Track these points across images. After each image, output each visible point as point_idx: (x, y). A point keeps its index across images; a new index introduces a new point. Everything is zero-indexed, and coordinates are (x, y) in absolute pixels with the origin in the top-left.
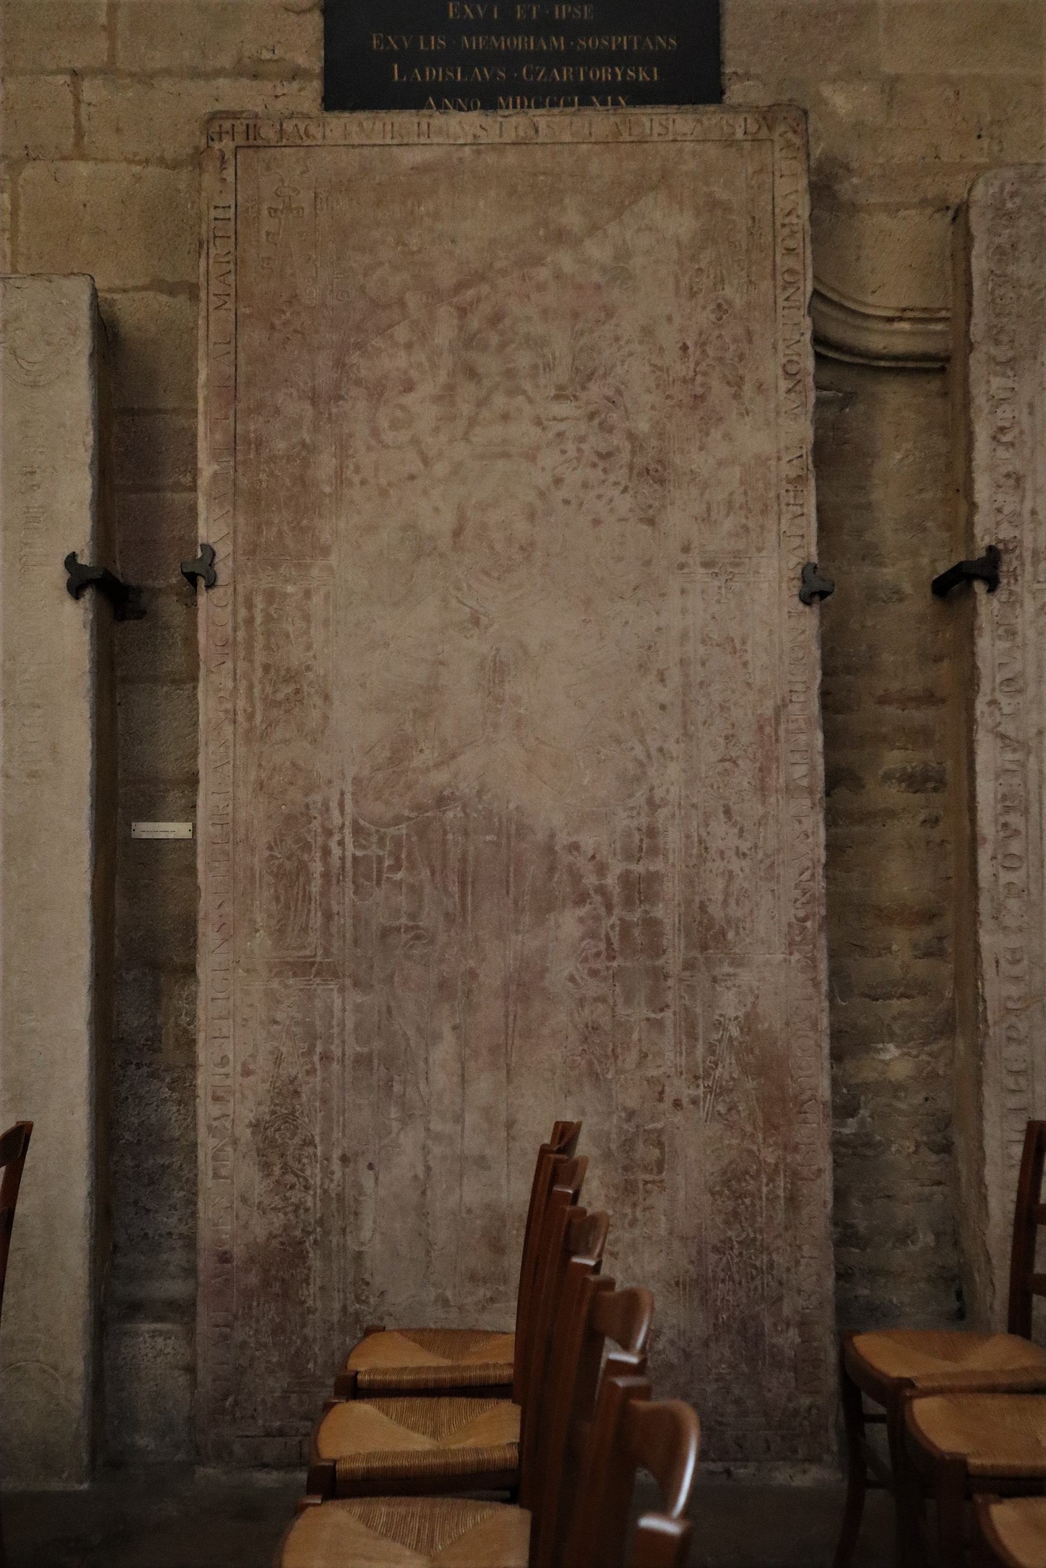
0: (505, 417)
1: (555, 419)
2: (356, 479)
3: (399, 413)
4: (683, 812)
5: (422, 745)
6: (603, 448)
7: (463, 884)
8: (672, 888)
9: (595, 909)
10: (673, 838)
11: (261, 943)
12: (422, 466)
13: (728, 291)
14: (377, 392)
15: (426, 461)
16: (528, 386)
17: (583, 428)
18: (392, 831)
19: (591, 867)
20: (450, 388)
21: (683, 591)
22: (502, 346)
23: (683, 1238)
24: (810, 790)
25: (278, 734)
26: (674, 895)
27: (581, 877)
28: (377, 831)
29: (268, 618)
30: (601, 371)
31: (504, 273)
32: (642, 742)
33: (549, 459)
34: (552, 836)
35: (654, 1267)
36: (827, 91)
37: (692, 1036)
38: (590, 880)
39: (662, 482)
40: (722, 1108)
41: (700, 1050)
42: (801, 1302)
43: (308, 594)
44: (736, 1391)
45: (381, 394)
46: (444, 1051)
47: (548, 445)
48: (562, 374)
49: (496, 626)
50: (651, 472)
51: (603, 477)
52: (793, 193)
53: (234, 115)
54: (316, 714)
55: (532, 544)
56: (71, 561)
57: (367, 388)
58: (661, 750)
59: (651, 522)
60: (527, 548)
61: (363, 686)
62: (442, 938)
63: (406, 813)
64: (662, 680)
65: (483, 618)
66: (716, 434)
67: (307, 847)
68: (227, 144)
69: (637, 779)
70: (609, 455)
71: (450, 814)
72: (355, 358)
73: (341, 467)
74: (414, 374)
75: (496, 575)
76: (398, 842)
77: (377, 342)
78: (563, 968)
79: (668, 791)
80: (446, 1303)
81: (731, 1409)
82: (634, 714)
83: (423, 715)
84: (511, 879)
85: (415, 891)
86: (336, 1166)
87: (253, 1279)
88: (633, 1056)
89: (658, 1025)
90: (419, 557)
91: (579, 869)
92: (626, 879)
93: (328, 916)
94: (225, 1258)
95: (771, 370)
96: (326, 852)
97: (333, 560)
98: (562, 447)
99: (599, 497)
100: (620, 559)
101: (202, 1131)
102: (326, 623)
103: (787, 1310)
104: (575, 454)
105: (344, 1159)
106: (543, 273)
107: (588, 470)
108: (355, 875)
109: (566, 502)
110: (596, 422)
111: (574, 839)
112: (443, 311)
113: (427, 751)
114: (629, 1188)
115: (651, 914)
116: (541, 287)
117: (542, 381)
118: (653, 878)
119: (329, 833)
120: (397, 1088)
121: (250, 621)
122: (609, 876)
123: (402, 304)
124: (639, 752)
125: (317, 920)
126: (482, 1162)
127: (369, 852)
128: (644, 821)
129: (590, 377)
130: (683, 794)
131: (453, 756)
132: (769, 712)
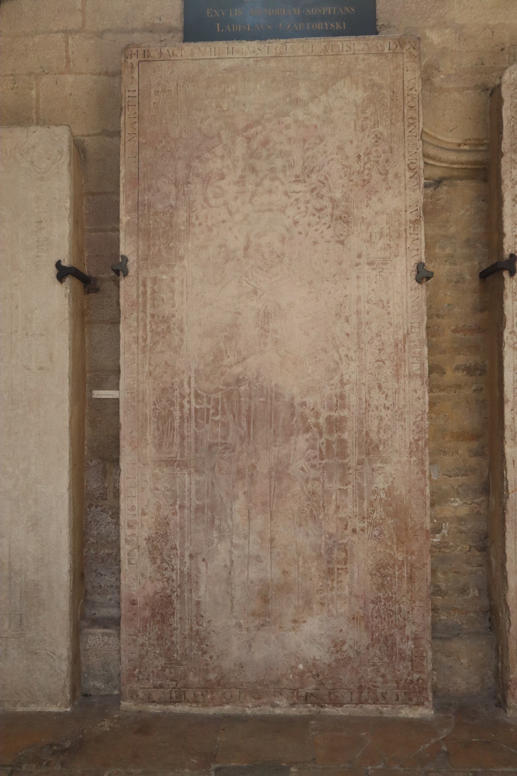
0: (270, 191)
1: (294, 192)
2: (197, 223)
3: (217, 190)
4: (358, 387)
5: (229, 354)
6: (318, 206)
7: (249, 422)
8: (352, 424)
9: (314, 435)
10: (352, 400)
11: (150, 451)
12: (229, 216)
13: (381, 128)
14: (206, 180)
15: (230, 213)
16: (281, 175)
17: (308, 196)
18: (214, 396)
19: (312, 414)
20: (243, 177)
21: (358, 277)
22: (269, 156)
23: (356, 596)
24: (421, 376)
25: (159, 347)
26: (353, 428)
27: (307, 418)
28: (207, 396)
29: (154, 292)
30: (318, 168)
31: (269, 120)
32: (338, 352)
33: (291, 212)
34: (293, 399)
35: (342, 610)
36: (428, 33)
37: (362, 498)
38: (312, 420)
39: (347, 222)
40: (376, 533)
41: (366, 504)
42: (414, 628)
43: (173, 280)
44: (382, 671)
45: (209, 181)
46: (240, 504)
47: (291, 205)
48: (298, 170)
49: (265, 295)
50: (343, 218)
51: (318, 220)
52: (412, 77)
53: (138, 46)
54: (177, 338)
55: (283, 254)
56: (58, 265)
57: (202, 178)
58: (347, 356)
59: (342, 243)
60: (280, 256)
61: (200, 324)
62: (238, 449)
63: (221, 387)
64: (348, 321)
65: (258, 290)
66: (374, 199)
67: (172, 404)
68: (134, 60)
69: (335, 370)
70: (321, 210)
71: (243, 388)
72: (196, 163)
73: (189, 218)
74: (224, 170)
75: (265, 269)
76: (217, 401)
77: (208, 155)
78: (298, 464)
79: (350, 376)
80: (240, 626)
81: (380, 679)
82: (333, 338)
83: (229, 339)
84: (273, 420)
85: (225, 425)
86: (187, 559)
87: (147, 613)
88: (333, 507)
89: (345, 492)
90: (227, 261)
91: (306, 415)
92: (329, 419)
93: (183, 438)
94: (134, 603)
95: (401, 167)
96: (182, 406)
97: (185, 262)
98: (298, 206)
99: (316, 230)
100: (326, 261)
101: (122, 542)
102: (182, 294)
103: (408, 632)
104: (305, 210)
105: (191, 556)
106: (288, 120)
107: (311, 217)
108: (196, 417)
109: (300, 233)
110: (315, 193)
111: (304, 400)
112: (239, 139)
113: (231, 357)
114: (330, 572)
115: (342, 437)
116: (288, 127)
117: (288, 174)
118: (343, 419)
119: (183, 397)
120: (217, 522)
121: (145, 293)
122: (321, 418)
123: (219, 136)
124: (336, 357)
125: (177, 440)
126: (258, 559)
127: (202, 406)
128: (338, 391)
129: (312, 171)
130: (358, 377)
131: (244, 359)
132: (401, 337)
